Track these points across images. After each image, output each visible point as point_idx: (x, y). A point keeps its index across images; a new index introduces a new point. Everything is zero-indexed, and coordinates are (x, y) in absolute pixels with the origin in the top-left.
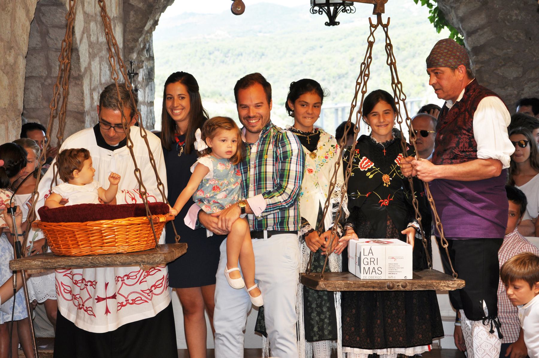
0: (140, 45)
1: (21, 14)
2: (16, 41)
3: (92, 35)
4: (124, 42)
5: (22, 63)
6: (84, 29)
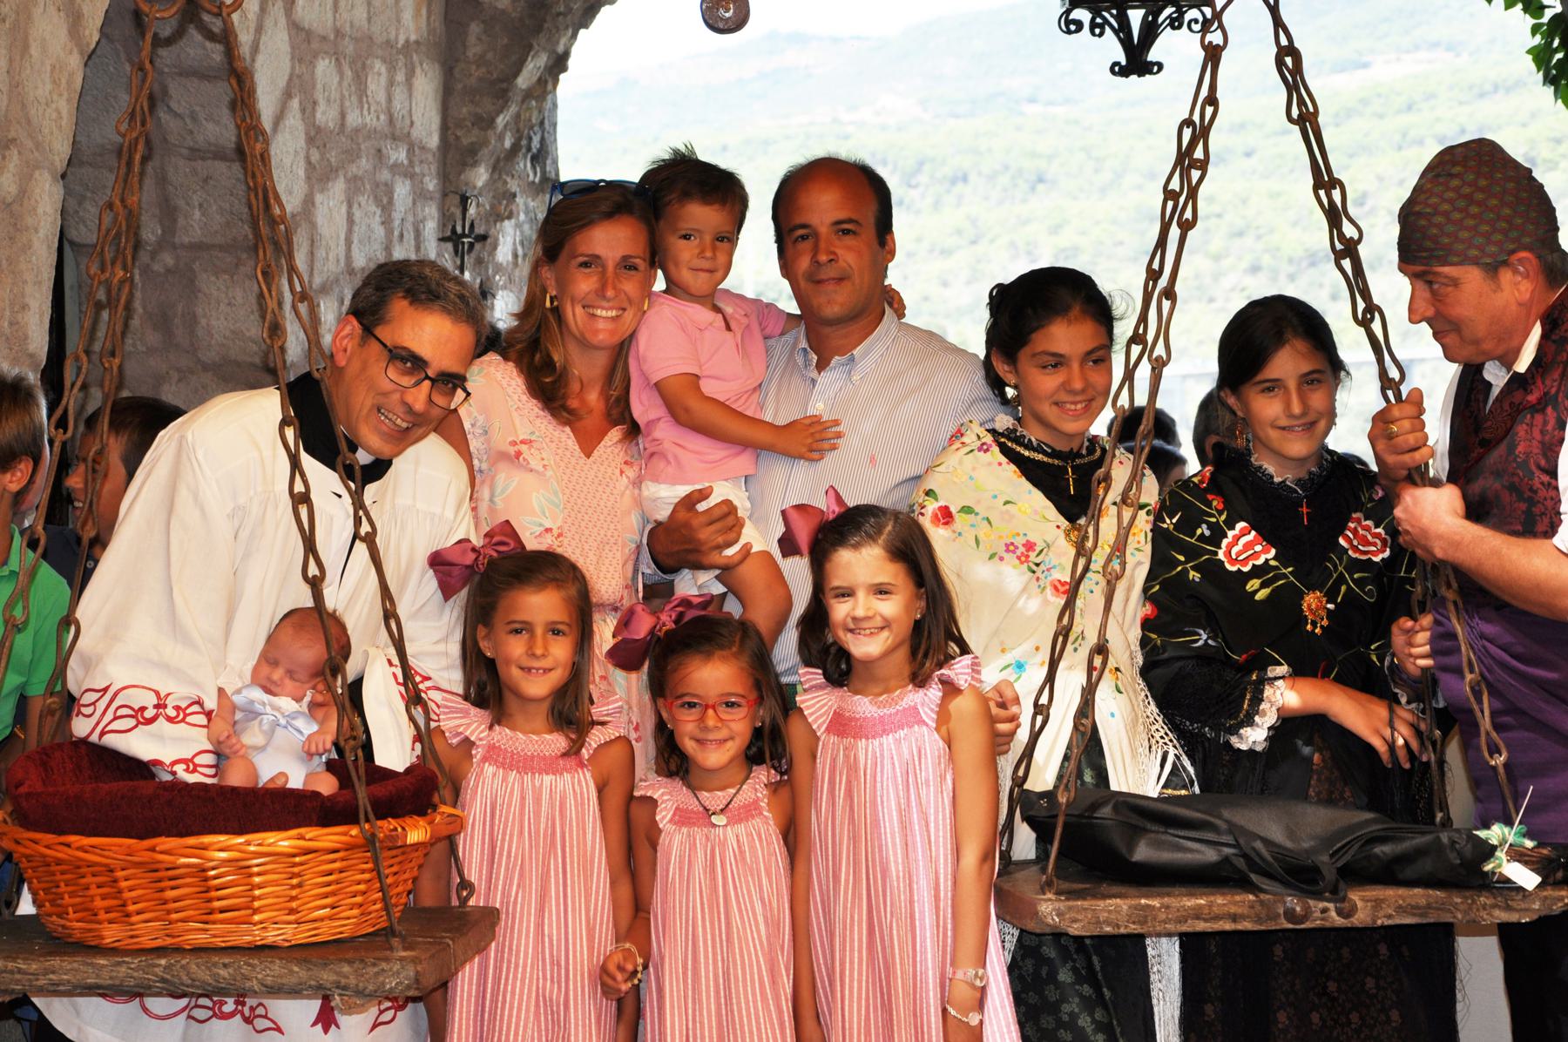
0: (501, 138)
4: (444, 128)
6: (290, 79)
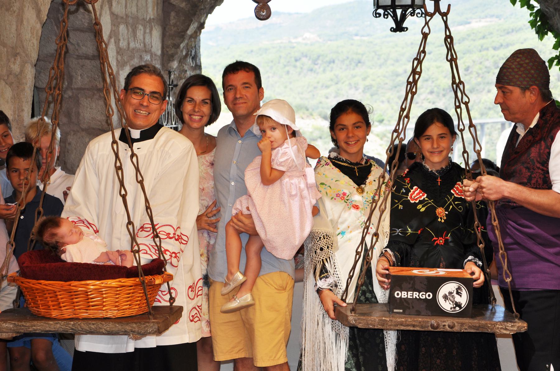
0: (182, 51)
1: (30, 15)
2: (23, 47)
3: (121, 39)
4: (163, 48)
5: (30, 73)
6: (111, 32)
